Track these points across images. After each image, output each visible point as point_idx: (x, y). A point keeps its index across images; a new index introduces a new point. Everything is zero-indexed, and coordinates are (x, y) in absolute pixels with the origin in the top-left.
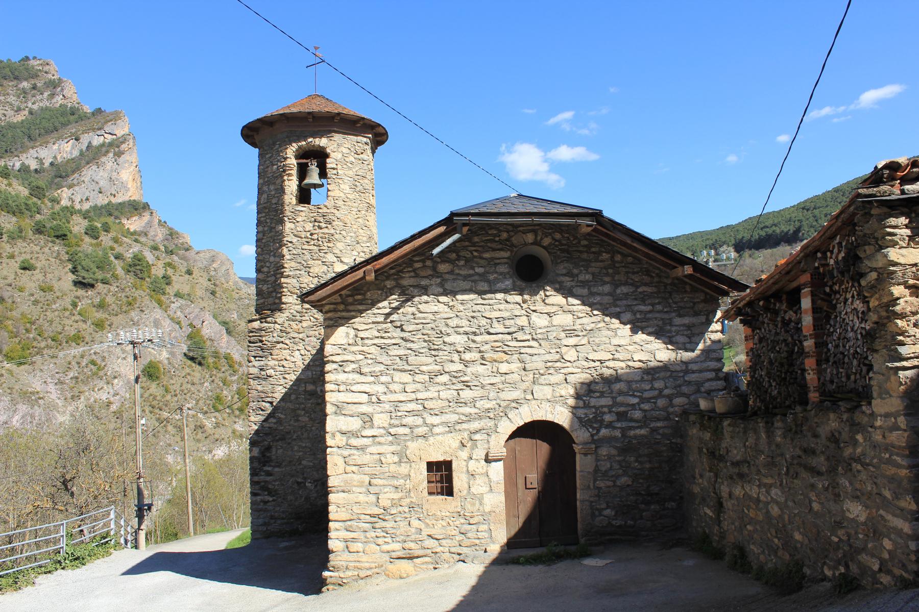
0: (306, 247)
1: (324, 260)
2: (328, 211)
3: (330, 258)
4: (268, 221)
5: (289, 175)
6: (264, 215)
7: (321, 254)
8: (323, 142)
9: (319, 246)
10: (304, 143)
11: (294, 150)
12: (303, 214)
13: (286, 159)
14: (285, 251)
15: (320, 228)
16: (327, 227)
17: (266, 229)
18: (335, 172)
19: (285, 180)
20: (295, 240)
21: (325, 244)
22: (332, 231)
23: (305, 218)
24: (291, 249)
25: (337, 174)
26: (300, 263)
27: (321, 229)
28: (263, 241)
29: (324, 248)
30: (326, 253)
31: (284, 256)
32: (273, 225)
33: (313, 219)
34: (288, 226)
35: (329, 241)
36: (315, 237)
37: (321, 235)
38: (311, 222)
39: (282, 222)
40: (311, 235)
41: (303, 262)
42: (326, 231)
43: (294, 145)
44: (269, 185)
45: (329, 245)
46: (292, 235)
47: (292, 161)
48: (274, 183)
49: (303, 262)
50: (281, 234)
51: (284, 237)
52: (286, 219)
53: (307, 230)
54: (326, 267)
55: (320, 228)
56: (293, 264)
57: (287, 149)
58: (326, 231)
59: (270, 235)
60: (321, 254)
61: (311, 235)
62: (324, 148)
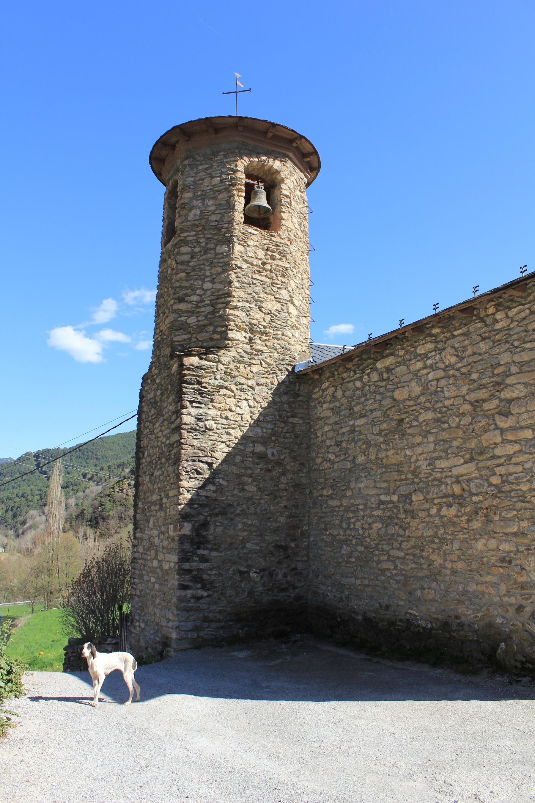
0: (256, 276)
1: (278, 296)
2: (283, 241)
3: (284, 294)
4: (202, 240)
5: (239, 190)
6: (194, 233)
7: (275, 289)
8: (277, 165)
9: (272, 279)
10: (256, 160)
11: (246, 164)
12: (256, 238)
13: (235, 172)
14: (233, 276)
15: (273, 259)
16: (280, 259)
17: (197, 250)
18: (288, 200)
19: (234, 195)
20: (245, 266)
21: (280, 278)
22: (288, 265)
23: (258, 244)
24: (240, 275)
25: (290, 203)
26: (251, 294)
27: (274, 260)
28: (191, 264)
29: (278, 282)
30: (279, 288)
31: (231, 282)
32: (211, 246)
33: (266, 247)
34: (238, 248)
35: (283, 276)
36: (268, 267)
37: (274, 267)
38: (262, 249)
39: (229, 242)
40: (264, 264)
41: (254, 294)
42: (280, 263)
43: (245, 158)
44: (203, 200)
45: (284, 280)
46: (241, 259)
47: (241, 176)
48: (215, 198)
49: (254, 294)
50: (229, 255)
51: (232, 259)
52: (235, 239)
53: (259, 257)
54: (279, 305)
55: (273, 259)
56: (242, 294)
57: (237, 161)
58: (280, 263)
59: (204, 257)
60: (275, 289)
61: (264, 264)
62: (278, 172)
